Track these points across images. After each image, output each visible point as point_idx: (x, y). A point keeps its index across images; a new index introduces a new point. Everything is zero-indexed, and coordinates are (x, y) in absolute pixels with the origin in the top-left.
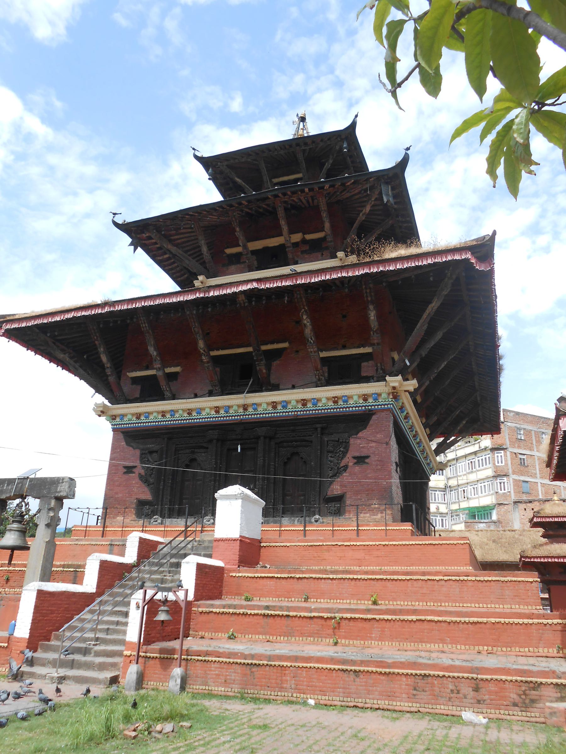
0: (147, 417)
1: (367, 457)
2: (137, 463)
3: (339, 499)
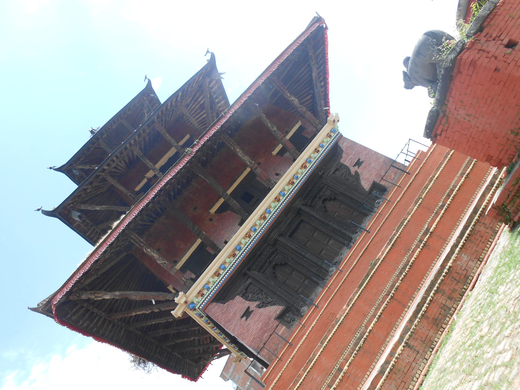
0: (224, 269)
2: (247, 304)
3: (375, 186)
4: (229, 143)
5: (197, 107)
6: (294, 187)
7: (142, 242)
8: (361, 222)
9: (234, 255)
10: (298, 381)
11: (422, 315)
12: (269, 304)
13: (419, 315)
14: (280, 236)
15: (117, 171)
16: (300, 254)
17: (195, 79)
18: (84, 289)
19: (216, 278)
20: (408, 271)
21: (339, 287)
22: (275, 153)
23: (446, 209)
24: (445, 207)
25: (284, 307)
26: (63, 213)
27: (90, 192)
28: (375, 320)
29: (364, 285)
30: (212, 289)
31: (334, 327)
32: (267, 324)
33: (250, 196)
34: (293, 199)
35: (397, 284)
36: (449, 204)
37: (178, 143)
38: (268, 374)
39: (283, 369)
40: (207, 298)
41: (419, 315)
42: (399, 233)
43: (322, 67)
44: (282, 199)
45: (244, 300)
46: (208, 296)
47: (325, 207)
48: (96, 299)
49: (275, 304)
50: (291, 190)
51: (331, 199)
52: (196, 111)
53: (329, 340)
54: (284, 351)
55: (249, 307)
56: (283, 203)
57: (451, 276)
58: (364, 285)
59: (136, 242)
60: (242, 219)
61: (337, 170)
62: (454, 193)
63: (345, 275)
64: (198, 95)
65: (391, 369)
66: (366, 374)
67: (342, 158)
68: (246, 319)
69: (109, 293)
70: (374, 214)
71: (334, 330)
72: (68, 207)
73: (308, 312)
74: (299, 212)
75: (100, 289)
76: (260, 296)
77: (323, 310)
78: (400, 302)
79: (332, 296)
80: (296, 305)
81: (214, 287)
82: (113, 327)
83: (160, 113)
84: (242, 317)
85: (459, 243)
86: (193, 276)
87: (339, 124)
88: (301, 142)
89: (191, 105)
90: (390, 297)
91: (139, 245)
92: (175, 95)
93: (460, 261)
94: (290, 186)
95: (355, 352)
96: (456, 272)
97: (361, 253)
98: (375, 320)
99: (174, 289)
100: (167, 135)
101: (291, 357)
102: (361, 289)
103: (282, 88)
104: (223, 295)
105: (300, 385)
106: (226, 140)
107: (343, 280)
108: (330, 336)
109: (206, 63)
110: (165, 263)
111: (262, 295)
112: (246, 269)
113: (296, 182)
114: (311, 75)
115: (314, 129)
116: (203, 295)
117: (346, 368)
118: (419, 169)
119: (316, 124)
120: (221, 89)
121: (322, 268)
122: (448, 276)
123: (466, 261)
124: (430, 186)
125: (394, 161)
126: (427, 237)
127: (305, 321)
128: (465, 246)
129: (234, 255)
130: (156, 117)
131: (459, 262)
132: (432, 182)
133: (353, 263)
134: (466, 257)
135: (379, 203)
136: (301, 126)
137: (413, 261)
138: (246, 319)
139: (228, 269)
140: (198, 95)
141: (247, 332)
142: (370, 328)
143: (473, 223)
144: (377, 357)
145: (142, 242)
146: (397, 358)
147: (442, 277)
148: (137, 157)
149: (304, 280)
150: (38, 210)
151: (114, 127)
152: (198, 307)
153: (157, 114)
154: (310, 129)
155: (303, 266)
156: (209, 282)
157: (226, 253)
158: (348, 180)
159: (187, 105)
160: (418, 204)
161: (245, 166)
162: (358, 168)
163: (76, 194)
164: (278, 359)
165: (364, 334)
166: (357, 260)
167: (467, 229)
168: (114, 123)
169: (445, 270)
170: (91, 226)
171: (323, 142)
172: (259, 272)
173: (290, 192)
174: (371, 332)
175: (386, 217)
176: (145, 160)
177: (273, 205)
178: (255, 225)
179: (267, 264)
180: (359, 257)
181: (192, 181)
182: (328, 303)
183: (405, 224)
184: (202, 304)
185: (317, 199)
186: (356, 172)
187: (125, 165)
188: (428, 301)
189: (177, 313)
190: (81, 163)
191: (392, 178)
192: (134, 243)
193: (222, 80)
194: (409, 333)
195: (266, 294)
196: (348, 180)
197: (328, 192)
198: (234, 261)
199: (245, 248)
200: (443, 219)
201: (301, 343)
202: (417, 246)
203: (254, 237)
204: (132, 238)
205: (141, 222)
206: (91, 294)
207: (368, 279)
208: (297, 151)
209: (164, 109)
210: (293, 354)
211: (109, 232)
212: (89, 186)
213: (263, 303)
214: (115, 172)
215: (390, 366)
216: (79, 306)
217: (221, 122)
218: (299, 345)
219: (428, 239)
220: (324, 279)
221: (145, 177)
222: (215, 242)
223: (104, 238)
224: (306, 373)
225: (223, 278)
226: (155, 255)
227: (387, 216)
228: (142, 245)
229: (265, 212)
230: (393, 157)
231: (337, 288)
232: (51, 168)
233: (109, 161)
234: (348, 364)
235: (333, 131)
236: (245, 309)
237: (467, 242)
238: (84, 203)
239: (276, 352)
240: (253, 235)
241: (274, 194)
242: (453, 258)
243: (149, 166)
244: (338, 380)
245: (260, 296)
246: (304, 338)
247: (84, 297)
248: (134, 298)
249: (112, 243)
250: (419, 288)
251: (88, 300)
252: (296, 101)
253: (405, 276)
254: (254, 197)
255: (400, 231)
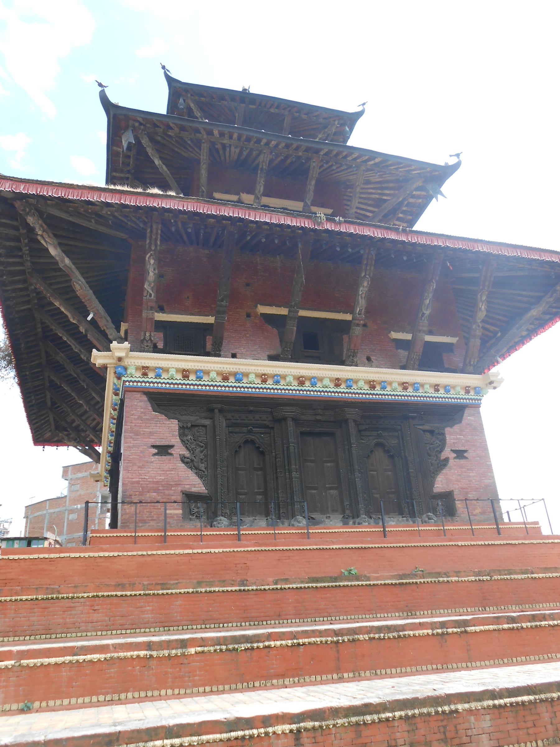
0: (199, 378)
1: (465, 451)
2: (176, 441)
3: (448, 497)
4: (367, 264)
5: (373, 196)
6: (369, 392)
7: (156, 246)
8: (388, 513)
9: (225, 379)
10: (123, 588)
11: (357, 724)
12: (196, 469)
13: (354, 719)
14: (293, 419)
15: (221, 152)
16: (289, 464)
17: (410, 166)
18: (41, 214)
19: (179, 376)
20: (389, 638)
21: (288, 548)
22: (394, 335)
23: (513, 629)
24: (514, 625)
25: (206, 491)
26: (120, 120)
27: (170, 136)
28: (289, 642)
29: (319, 585)
30: (162, 381)
31: (233, 585)
32: (169, 486)
33: (316, 344)
34: (352, 403)
35: (361, 637)
36: (522, 628)
37: (313, 204)
38: (105, 535)
39: (125, 554)
40: (145, 383)
41: (354, 719)
42: (422, 580)
43: (548, 317)
44: (343, 388)
45: (177, 433)
46: (150, 383)
47: (372, 452)
48: (39, 238)
49: (201, 477)
50: (362, 392)
51: (388, 452)
52: (368, 199)
53: (210, 592)
54: (150, 534)
55: (172, 446)
56: (338, 393)
57: (444, 723)
58: (319, 585)
59: (151, 237)
60: (279, 355)
61: (432, 432)
62: (543, 623)
63: (310, 545)
64: (391, 185)
65: (243, 737)
66: (204, 685)
67: (451, 427)
68: (155, 455)
69: (59, 250)
70: (411, 523)
71: (229, 589)
72: (131, 122)
73: (223, 528)
74: (342, 423)
75: (55, 235)
76: (198, 450)
77: (242, 549)
78: (338, 658)
79: (270, 548)
80: (220, 506)
81: (166, 381)
82: (21, 290)
83: (334, 153)
84: (154, 447)
85: (501, 698)
86: (160, 345)
87: (491, 392)
88: (432, 359)
89: (372, 186)
90: (335, 639)
91: (150, 244)
92: (372, 155)
93: (476, 720)
94: (367, 387)
95: (224, 647)
96: (456, 727)
97: (353, 546)
98: (289, 642)
99: (126, 332)
100: (313, 183)
101: (150, 553)
102: (310, 585)
103: (487, 283)
104: (165, 402)
105: (122, 596)
106: (367, 259)
107: (301, 548)
108: (217, 589)
109: (443, 164)
110: (150, 295)
111: (202, 452)
112: (219, 406)
113: (378, 390)
114: (527, 310)
115: (461, 365)
116: (145, 375)
117: (192, 651)
118: (520, 542)
119: (470, 362)
120: (421, 208)
121: (293, 504)
122: (441, 717)
123: (483, 729)
124: (516, 577)
125: (498, 500)
126: (455, 630)
127: (208, 533)
128: (502, 710)
129: (225, 379)
130: (326, 150)
131: (472, 719)
132: (523, 576)
133: (334, 543)
134: (489, 724)
135: (429, 519)
136: (451, 345)
137: (409, 635)
138: (155, 455)
139: (202, 383)
140: (391, 185)
141: (139, 467)
142: (272, 643)
143: (543, 696)
144: (239, 686)
145: (156, 246)
146: (267, 734)
147: (432, 710)
148: (258, 165)
149: (259, 493)
150: (100, 85)
151: (272, 110)
152: (126, 379)
153: (331, 148)
154: (457, 359)
155: (277, 478)
156: (167, 370)
157: (222, 366)
158: (430, 456)
159: (368, 182)
160: (481, 578)
161: (349, 309)
162: (455, 458)
163: (154, 118)
164: (133, 534)
165: (258, 642)
166: (341, 546)
167: (529, 694)
168: (278, 107)
169: (446, 708)
170: (129, 172)
171: (454, 387)
172: (228, 426)
173: (359, 391)
174: (268, 649)
175: (425, 544)
176: (261, 177)
177: (326, 382)
178: (284, 377)
179: (245, 429)
180: (347, 546)
181: (279, 255)
182: (256, 549)
183: (441, 579)
184: (133, 382)
185: (375, 433)
186: (447, 460)
187: (236, 157)
188: (383, 716)
189: (98, 358)
190: (197, 103)
191: (475, 512)
192: (148, 235)
193: (434, 199)
194: (317, 724)
195: (206, 456)
196: (430, 456)
197: (394, 442)
198: (218, 384)
199: (244, 385)
200: (496, 634)
201: (177, 552)
202: (433, 626)
203: (267, 386)
204: (151, 227)
205: (180, 224)
206: (41, 226)
207: (330, 584)
208: (417, 363)
209: (344, 154)
210: (155, 552)
211: (140, 190)
212: (177, 130)
213: (192, 461)
214: (217, 150)
215: (247, 732)
216: (15, 223)
217: (388, 234)
218: (172, 552)
219: (453, 633)
220: (280, 519)
221: (238, 194)
222: (225, 342)
223: (125, 188)
224: (142, 592)
225: (186, 385)
226: (151, 275)
227: (428, 544)
228: (153, 248)
229: (310, 379)
230: (502, 493)
231: (285, 548)
232: (163, 67)
233: (226, 130)
234: (199, 649)
235: (478, 391)
236: (167, 443)
237: (509, 709)
238: (152, 139)
239: (141, 525)
240: (270, 383)
241: (341, 373)
242: (474, 705)
243: (258, 188)
244: (166, 653)
245: (198, 450)
246: (186, 551)
247: (30, 220)
248: (77, 287)
249: (127, 206)
250: (378, 672)
251: (31, 230)
252: (482, 314)
253: (379, 639)
254: (317, 349)
255: (426, 580)
